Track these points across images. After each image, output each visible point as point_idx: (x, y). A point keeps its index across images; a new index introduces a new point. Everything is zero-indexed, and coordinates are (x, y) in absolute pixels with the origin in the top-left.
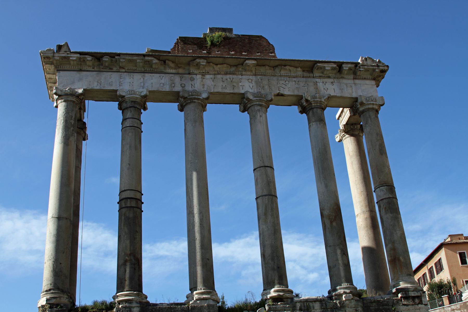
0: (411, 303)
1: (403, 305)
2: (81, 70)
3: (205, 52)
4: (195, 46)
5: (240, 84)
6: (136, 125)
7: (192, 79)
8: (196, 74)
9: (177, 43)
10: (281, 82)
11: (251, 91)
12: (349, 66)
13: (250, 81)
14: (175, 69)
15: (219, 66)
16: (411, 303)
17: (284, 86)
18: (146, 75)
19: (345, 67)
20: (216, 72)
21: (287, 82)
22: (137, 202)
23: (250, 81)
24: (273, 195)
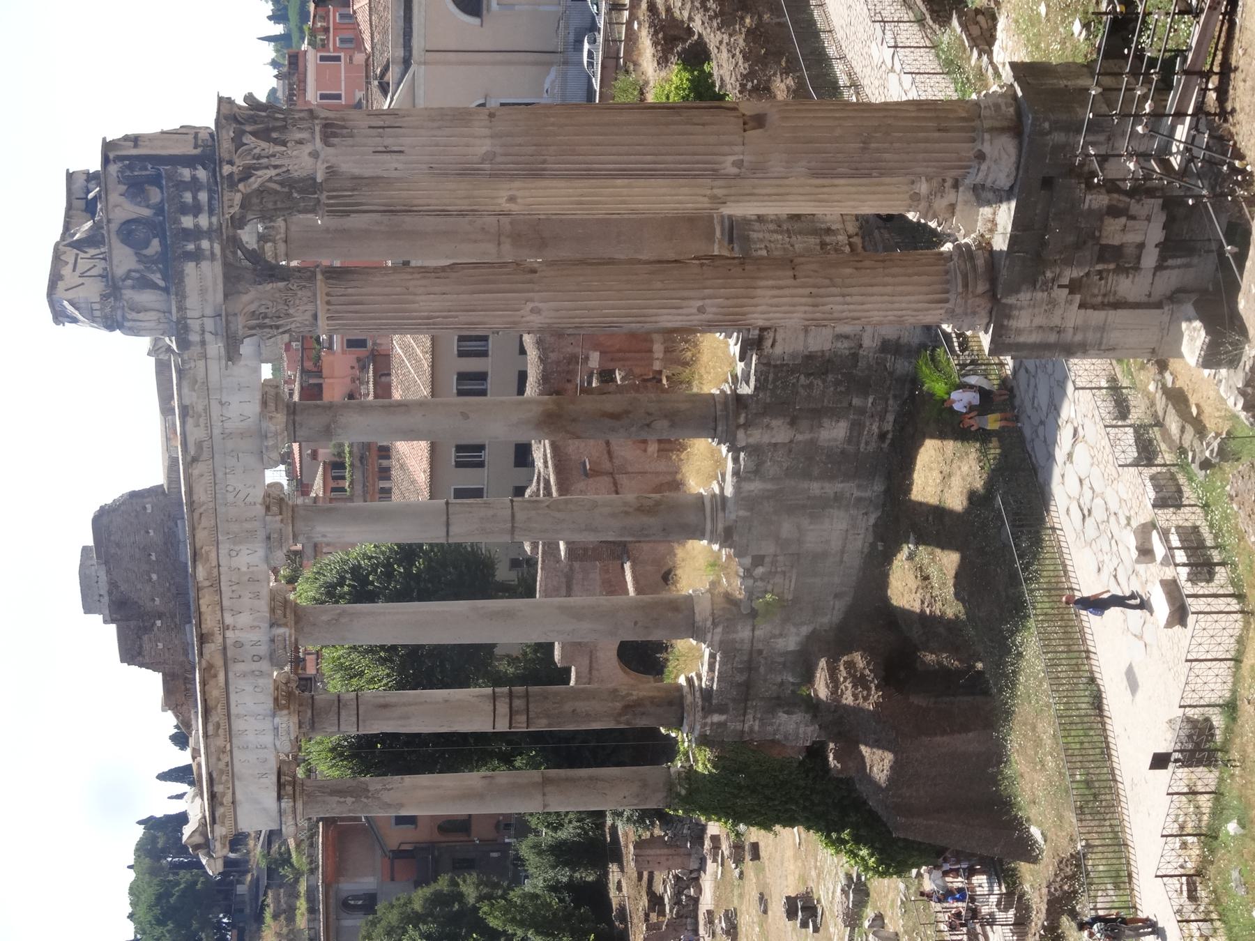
0: (771, 334)
1: (772, 346)
2: (233, 803)
3: (159, 623)
4: (146, 638)
5: (244, 569)
6: (354, 719)
7: (239, 645)
8: (224, 637)
9: (141, 666)
10: (230, 497)
11: (261, 553)
12: (185, 391)
13: (234, 553)
14: (215, 676)
15: (203, 609)
16: (771, 334)
17: (242, 495)
18: (234, 710)
19: (191, 398)
20: (218, 608)
21: (230, 489)
22: (518, 712)
23: (234, 553)
24: (513, 527)
